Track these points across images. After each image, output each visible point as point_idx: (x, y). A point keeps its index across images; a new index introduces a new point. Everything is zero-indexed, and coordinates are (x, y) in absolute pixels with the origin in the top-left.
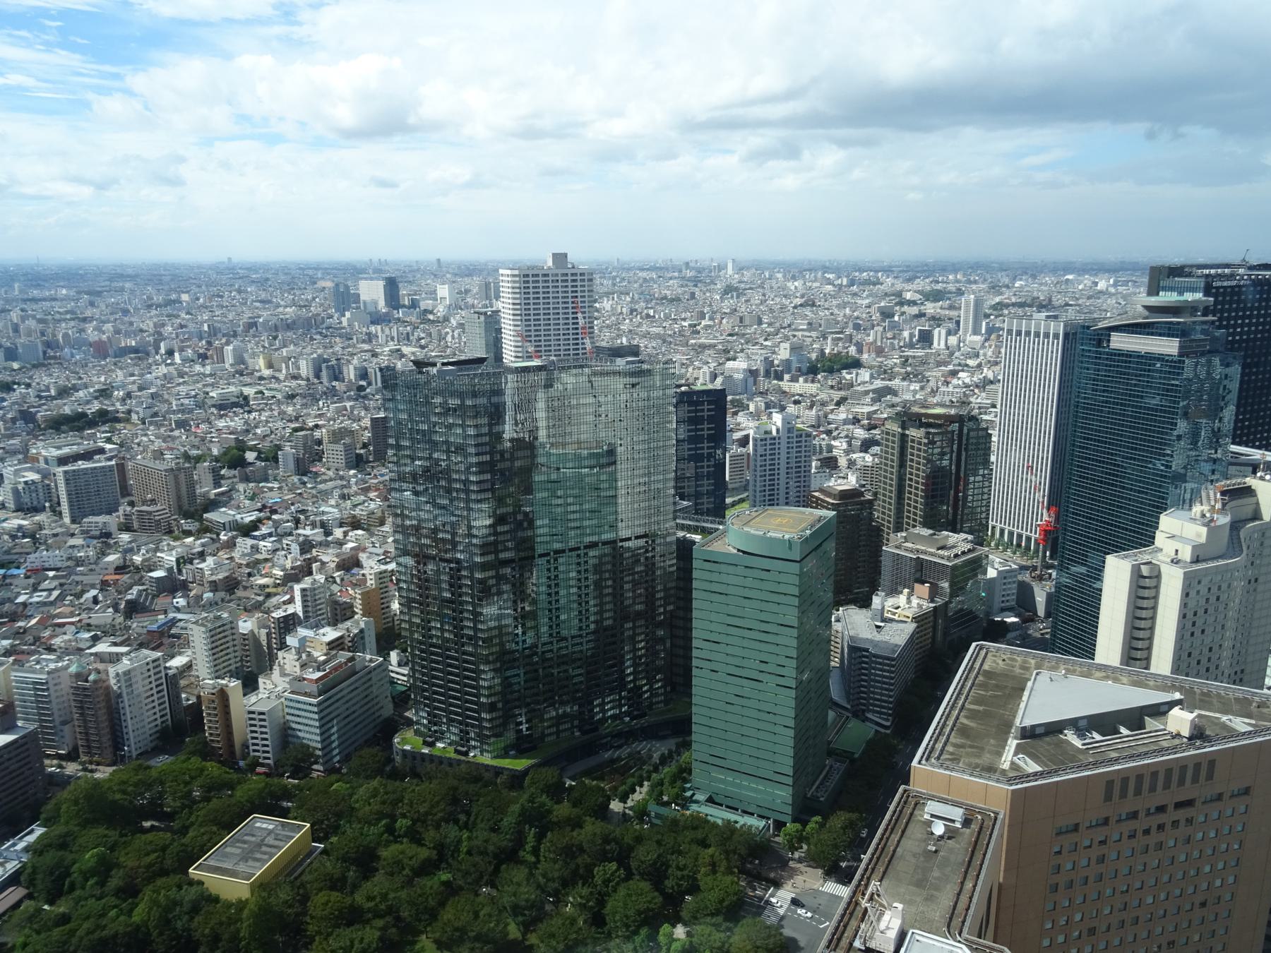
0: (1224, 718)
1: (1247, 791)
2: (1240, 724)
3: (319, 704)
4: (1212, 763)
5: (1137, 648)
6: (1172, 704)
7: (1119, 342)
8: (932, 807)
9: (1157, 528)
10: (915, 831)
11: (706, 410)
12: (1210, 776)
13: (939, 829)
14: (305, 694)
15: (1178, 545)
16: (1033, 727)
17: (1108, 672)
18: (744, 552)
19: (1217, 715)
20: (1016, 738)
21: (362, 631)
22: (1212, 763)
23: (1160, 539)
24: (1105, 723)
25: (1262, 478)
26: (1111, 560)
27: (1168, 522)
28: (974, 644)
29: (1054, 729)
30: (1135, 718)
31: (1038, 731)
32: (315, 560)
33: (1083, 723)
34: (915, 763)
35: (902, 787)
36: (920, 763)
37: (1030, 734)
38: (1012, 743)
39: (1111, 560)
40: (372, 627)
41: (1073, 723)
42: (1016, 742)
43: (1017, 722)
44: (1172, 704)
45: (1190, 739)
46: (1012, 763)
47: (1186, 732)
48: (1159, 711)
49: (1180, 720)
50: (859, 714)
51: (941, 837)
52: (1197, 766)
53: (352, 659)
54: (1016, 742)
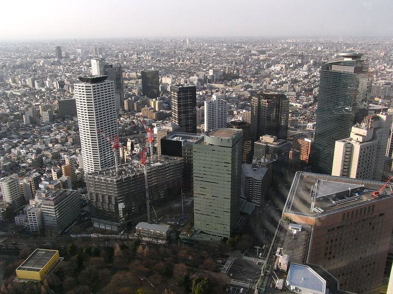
1: (381, 215)
3: (55, 208)
4: (374, 206)
7: (335, 68)
11: (189, 94)
12: (373, 210)
14: (49, 205)
18: (211, 145)
21: (66, 181)
23: (352, 135)
25: (382, 114)
26: (337, 142)
27: (354, 130)
32: (44, 155)
39: (337, 142)
40: (70, 179)
50: (249, 200)
53: (65, 191)
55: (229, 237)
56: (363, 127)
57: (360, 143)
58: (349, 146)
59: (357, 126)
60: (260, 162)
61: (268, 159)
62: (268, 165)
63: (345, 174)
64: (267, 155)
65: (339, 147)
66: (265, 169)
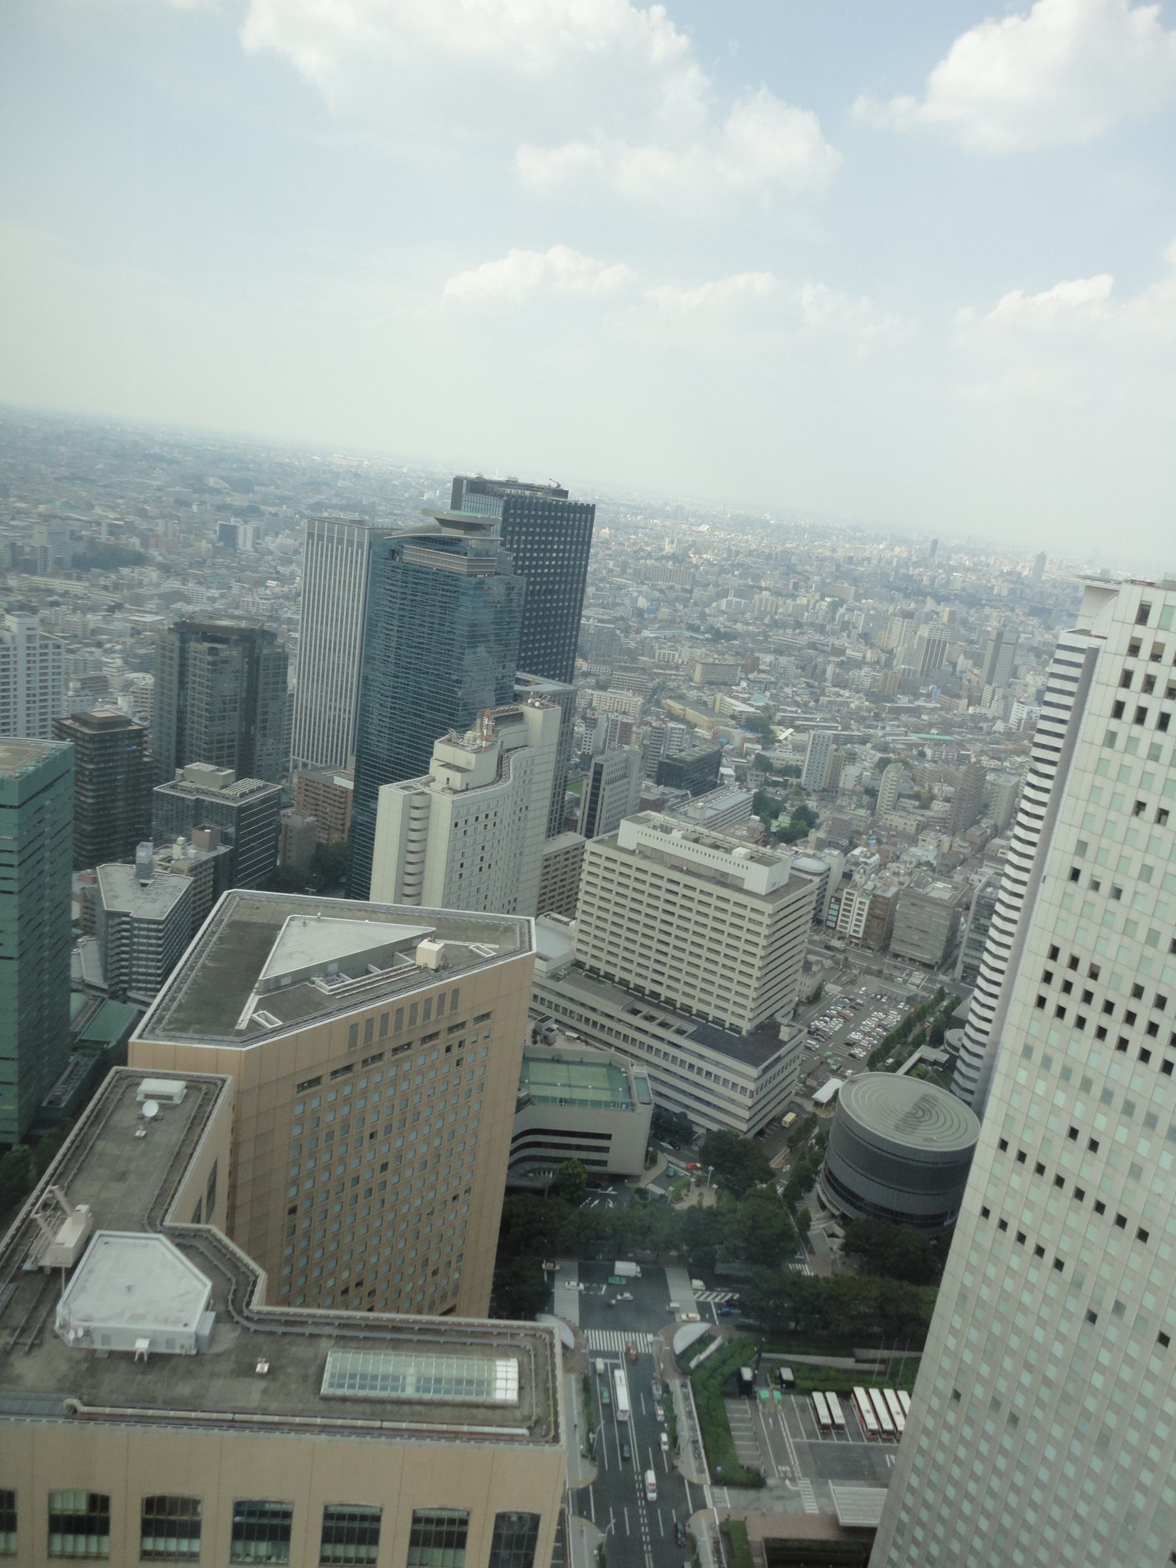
0: (472, 946)
1: (486, 1016)
2: (487, 949)
4: (456, 992)
5: (411, 886)
6: (422, 937)
8: (149, 1085)
9: (432, 754)
10: (123, 1118)
12: (454, 1006)
13: (151, 1109)
15: (449, 773)
16: (278, 979)
17: (374, 914)
19: (466, 944)
20: (257, 993)
22: (456, 992)
23: (434, 767)
24: (355, 965)
25: (533, 705)
27: (442, 750)
28: (226, 893)
29: (302, 977)
30: (386, 955)
31: (284, 982)
33: (333, 968)
34: (133, 1039)
35: (115, 1068)
36: (140, 1037)
37: (275, 985)
38: (253, 1000)
41: (322, 969)
42: (258, 997)
43: (261, 978)
44: (422, 937)
45: (436, 971)
46: (252, 1021)
47: (433, 965)
48: (408, 946)
49: (429, 951)
51: (155, 1119)
52: (442, 997)
54: (258, 997)
55: (13, 1139)
56: (465, 742)
57: (456, 792)
58: (418, 801)
59: (450, 740)
60: (169, 859)
61: (199, 847)
62: (193, 870)
63: (409, 890)
64: (195, 833)
65: (391, 799)
66: (184, 883)
